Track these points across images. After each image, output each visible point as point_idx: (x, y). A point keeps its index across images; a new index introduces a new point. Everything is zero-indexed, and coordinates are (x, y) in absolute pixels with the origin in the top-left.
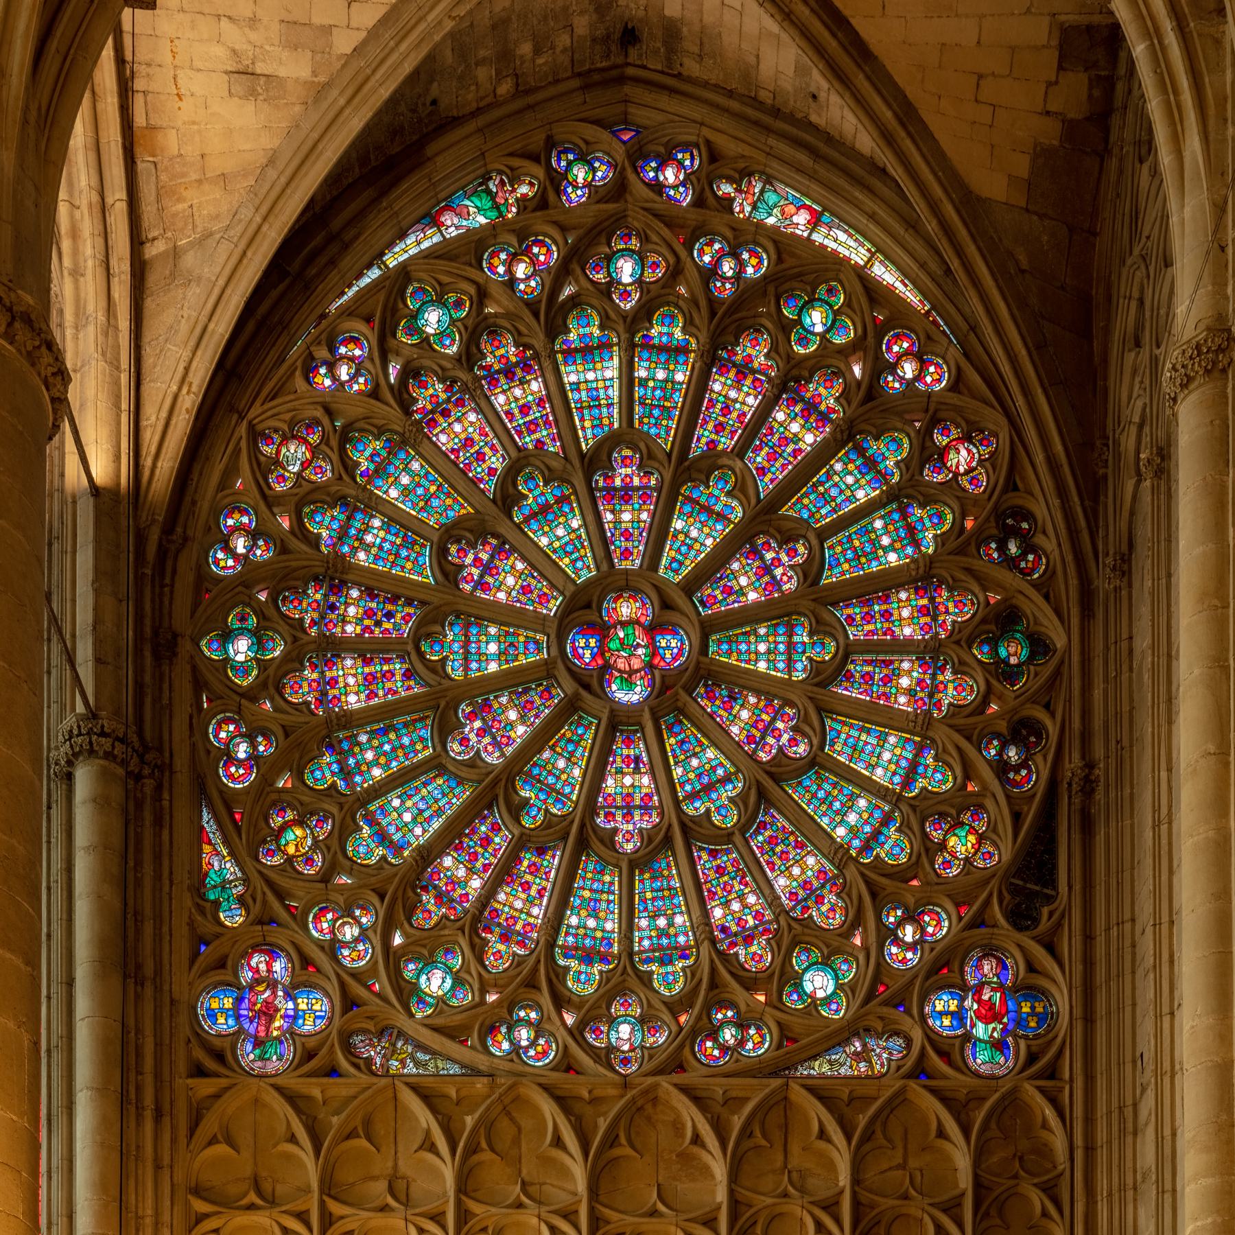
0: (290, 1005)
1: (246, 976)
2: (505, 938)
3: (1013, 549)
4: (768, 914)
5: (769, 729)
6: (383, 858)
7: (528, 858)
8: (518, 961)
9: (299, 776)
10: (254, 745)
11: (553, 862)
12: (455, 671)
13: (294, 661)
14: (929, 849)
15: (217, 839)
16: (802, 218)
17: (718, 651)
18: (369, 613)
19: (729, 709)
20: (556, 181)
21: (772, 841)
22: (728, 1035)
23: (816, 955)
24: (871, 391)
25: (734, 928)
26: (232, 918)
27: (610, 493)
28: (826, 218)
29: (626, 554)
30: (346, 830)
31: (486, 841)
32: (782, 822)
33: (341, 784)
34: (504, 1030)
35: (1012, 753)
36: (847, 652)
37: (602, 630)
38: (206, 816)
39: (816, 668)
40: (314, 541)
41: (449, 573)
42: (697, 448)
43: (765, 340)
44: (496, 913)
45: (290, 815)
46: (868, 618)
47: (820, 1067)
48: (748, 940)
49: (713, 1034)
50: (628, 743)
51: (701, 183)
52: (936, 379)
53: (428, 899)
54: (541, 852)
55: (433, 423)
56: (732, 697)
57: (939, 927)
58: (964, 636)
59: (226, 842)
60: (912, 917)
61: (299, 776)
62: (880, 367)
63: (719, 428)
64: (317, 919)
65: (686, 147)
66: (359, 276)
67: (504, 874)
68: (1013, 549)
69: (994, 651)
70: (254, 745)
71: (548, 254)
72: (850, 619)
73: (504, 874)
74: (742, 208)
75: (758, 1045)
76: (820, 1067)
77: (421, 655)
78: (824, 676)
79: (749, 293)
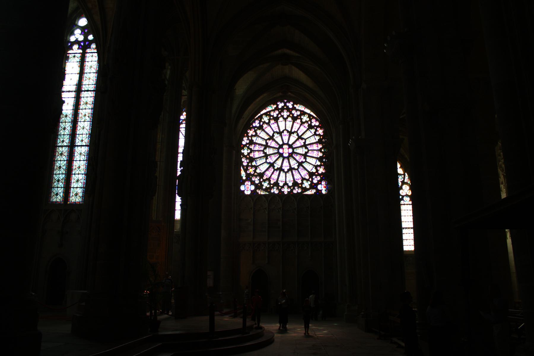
0: (250, 187)
1: (246, 184)
2: (273, 180)
3: (326, 140)
4: (301, 177)
5: (301, 158)
6: (260, 172)
7: (275, 172)
8: (274, 182)
9: (251, 164)
10: (247, 161)
11: (278, 172)
12: (268, 153)
13: (251, 152)
14: (317, 171)
15: (243, 170)
16: (304, 108)
17: (295, 151)
18: (259, 147)
19: (296, 156)
20: (278, 105)
21: (301, 170)
22: (297, 190)
23: (306, 181)
24: (311, 124)
25: (297, 179)
26: (244, 178)
27: (284, 135)
28: (306, 108)
29: (286, 141)
30: (256, 169)
31: (271, 170)
32: (302, 168)
33: (256, 165)
34: (273, 189)
35: (326, 160)
36: (309, 150)
37: (283, 149)
38: (242, 168)
39: (306, 152)
40: (253, 140)
41: (267, 143)
42: (293, 131)
43: (300, 120)
44: (272, 177)
45: (251, 168)
46: (311, 147)
47: (306, 193)
48: (299, 180)
49: (295, 189)
50: (286, 160)
51: (293, 105)
52: (317, 124)
53: (265, 176)
54: (277, 171)
55: (265, 129)
56: (297, 155)
57: (319, 178)
58: (321, 149)
59: (244, 170)
60: (316, 177)
61: (251, 164)
62: (311, 122)
63: (295, 129)
64: (253, 178)
65: (291, 102)
66: (258, 114)
67: (273, 173)
68: (326, 140)
69: (324, 150)
70: (247, 161)
71: (277, 112)
72: (309, 147)
73: (273, 173)
74: (297, 108)
75: (300, 191)
76: (306, 193)
77: (264, 151)
78: (306, 153)
79: (298, 116)
